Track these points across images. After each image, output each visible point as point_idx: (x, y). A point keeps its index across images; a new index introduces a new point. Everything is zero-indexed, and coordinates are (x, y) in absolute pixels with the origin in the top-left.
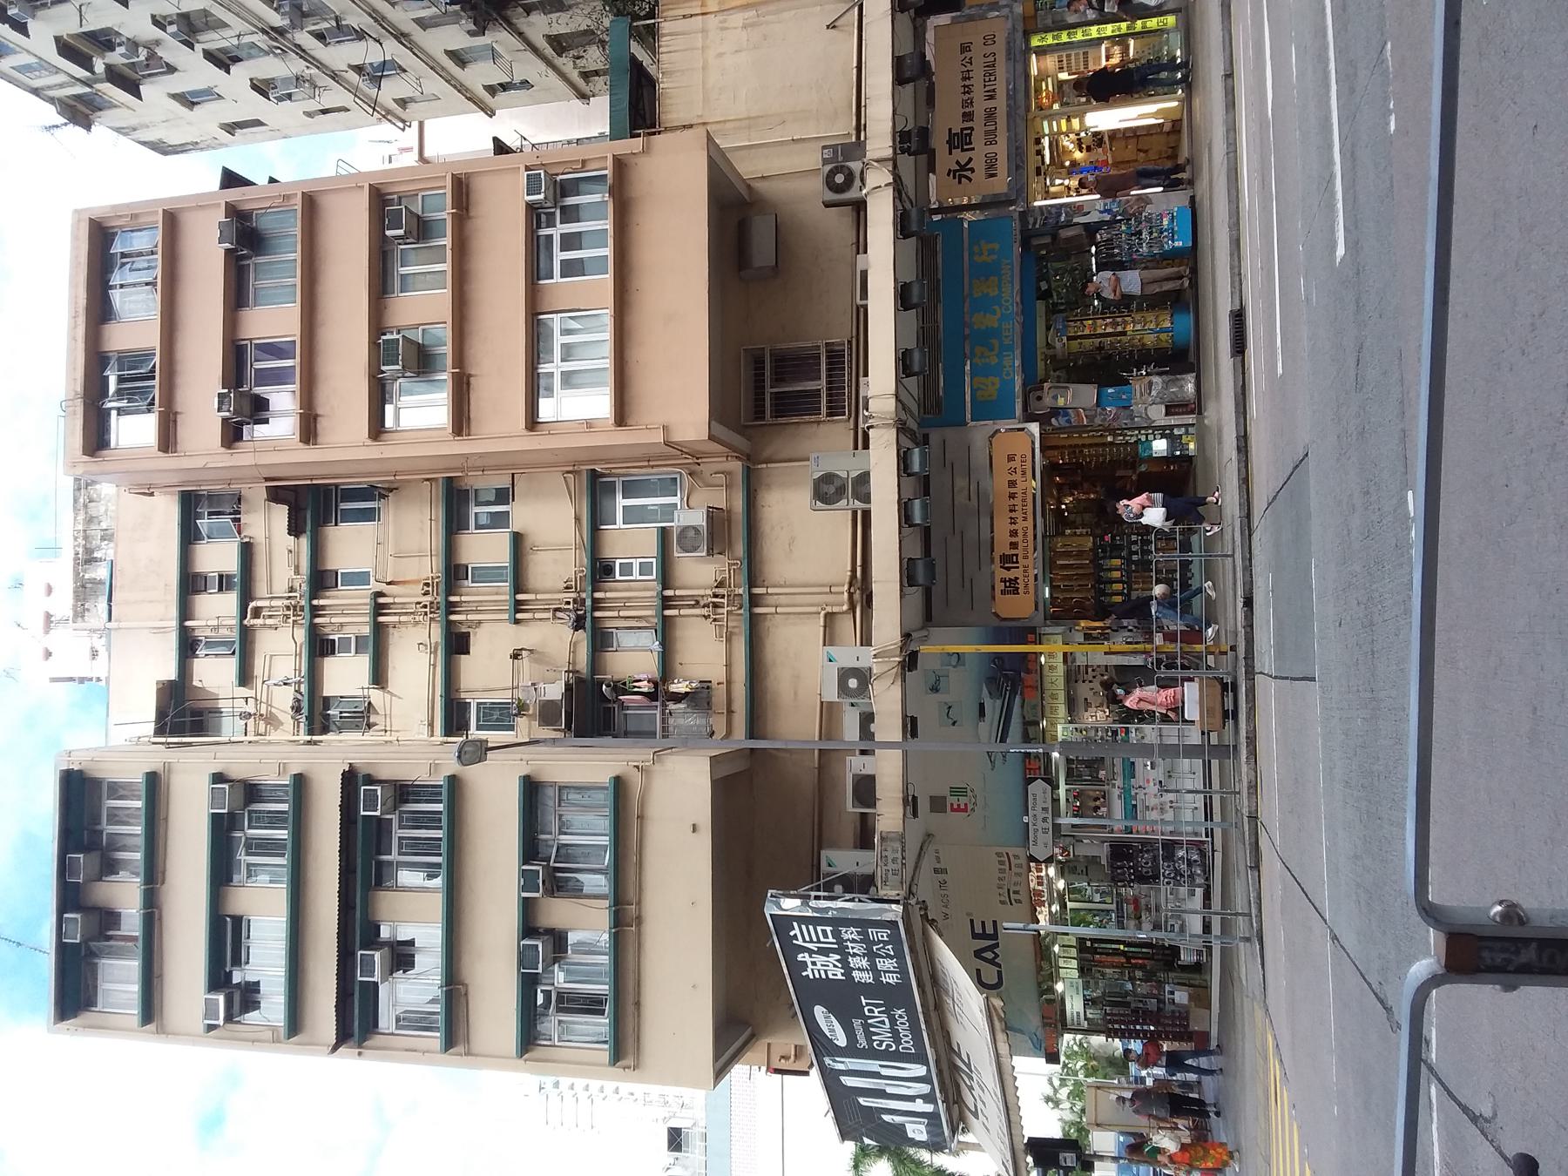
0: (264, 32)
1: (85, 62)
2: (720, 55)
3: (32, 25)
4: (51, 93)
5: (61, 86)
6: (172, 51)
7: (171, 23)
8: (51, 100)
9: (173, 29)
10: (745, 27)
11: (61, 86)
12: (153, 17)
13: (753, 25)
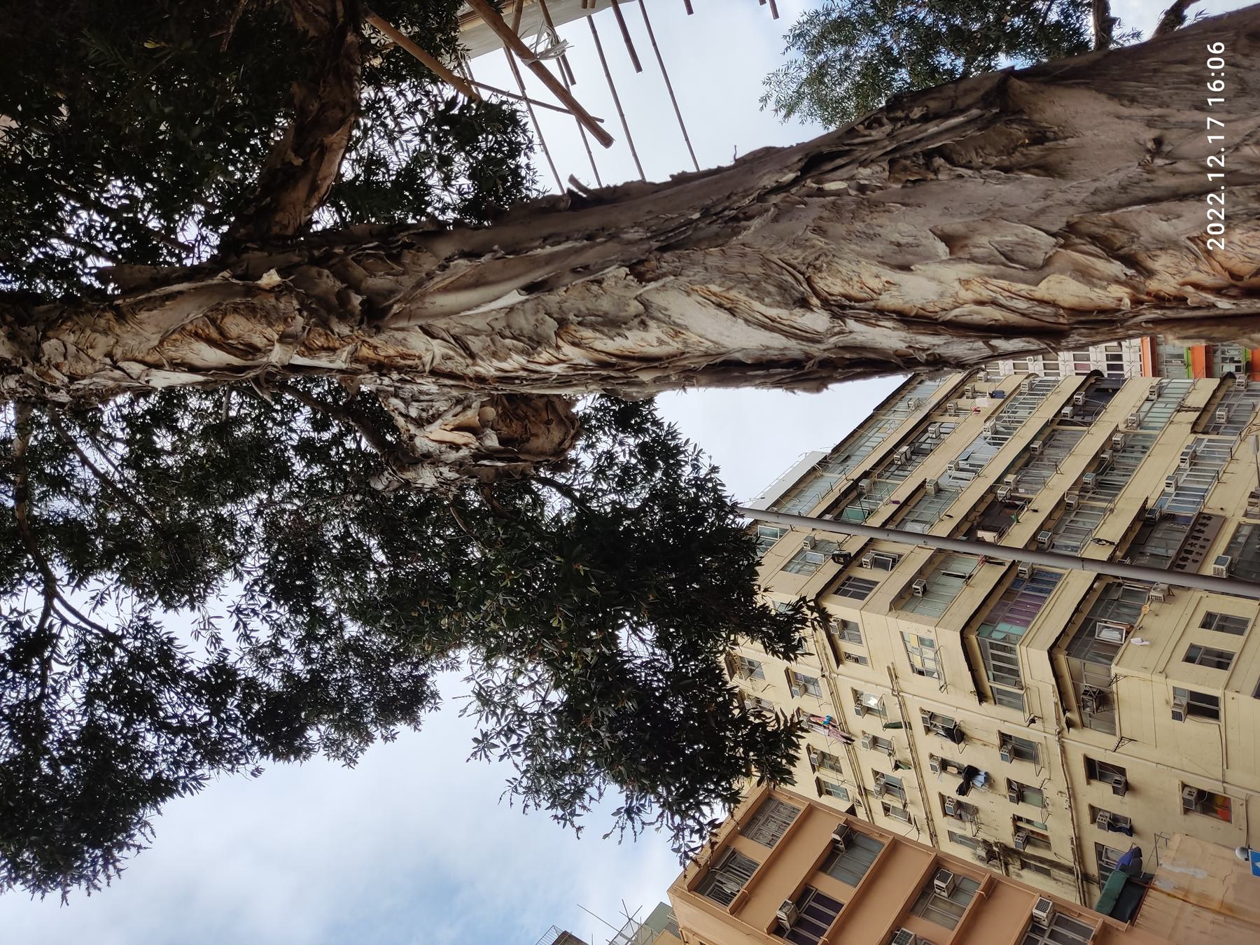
9: (813, 756)
10: (1213, 922)
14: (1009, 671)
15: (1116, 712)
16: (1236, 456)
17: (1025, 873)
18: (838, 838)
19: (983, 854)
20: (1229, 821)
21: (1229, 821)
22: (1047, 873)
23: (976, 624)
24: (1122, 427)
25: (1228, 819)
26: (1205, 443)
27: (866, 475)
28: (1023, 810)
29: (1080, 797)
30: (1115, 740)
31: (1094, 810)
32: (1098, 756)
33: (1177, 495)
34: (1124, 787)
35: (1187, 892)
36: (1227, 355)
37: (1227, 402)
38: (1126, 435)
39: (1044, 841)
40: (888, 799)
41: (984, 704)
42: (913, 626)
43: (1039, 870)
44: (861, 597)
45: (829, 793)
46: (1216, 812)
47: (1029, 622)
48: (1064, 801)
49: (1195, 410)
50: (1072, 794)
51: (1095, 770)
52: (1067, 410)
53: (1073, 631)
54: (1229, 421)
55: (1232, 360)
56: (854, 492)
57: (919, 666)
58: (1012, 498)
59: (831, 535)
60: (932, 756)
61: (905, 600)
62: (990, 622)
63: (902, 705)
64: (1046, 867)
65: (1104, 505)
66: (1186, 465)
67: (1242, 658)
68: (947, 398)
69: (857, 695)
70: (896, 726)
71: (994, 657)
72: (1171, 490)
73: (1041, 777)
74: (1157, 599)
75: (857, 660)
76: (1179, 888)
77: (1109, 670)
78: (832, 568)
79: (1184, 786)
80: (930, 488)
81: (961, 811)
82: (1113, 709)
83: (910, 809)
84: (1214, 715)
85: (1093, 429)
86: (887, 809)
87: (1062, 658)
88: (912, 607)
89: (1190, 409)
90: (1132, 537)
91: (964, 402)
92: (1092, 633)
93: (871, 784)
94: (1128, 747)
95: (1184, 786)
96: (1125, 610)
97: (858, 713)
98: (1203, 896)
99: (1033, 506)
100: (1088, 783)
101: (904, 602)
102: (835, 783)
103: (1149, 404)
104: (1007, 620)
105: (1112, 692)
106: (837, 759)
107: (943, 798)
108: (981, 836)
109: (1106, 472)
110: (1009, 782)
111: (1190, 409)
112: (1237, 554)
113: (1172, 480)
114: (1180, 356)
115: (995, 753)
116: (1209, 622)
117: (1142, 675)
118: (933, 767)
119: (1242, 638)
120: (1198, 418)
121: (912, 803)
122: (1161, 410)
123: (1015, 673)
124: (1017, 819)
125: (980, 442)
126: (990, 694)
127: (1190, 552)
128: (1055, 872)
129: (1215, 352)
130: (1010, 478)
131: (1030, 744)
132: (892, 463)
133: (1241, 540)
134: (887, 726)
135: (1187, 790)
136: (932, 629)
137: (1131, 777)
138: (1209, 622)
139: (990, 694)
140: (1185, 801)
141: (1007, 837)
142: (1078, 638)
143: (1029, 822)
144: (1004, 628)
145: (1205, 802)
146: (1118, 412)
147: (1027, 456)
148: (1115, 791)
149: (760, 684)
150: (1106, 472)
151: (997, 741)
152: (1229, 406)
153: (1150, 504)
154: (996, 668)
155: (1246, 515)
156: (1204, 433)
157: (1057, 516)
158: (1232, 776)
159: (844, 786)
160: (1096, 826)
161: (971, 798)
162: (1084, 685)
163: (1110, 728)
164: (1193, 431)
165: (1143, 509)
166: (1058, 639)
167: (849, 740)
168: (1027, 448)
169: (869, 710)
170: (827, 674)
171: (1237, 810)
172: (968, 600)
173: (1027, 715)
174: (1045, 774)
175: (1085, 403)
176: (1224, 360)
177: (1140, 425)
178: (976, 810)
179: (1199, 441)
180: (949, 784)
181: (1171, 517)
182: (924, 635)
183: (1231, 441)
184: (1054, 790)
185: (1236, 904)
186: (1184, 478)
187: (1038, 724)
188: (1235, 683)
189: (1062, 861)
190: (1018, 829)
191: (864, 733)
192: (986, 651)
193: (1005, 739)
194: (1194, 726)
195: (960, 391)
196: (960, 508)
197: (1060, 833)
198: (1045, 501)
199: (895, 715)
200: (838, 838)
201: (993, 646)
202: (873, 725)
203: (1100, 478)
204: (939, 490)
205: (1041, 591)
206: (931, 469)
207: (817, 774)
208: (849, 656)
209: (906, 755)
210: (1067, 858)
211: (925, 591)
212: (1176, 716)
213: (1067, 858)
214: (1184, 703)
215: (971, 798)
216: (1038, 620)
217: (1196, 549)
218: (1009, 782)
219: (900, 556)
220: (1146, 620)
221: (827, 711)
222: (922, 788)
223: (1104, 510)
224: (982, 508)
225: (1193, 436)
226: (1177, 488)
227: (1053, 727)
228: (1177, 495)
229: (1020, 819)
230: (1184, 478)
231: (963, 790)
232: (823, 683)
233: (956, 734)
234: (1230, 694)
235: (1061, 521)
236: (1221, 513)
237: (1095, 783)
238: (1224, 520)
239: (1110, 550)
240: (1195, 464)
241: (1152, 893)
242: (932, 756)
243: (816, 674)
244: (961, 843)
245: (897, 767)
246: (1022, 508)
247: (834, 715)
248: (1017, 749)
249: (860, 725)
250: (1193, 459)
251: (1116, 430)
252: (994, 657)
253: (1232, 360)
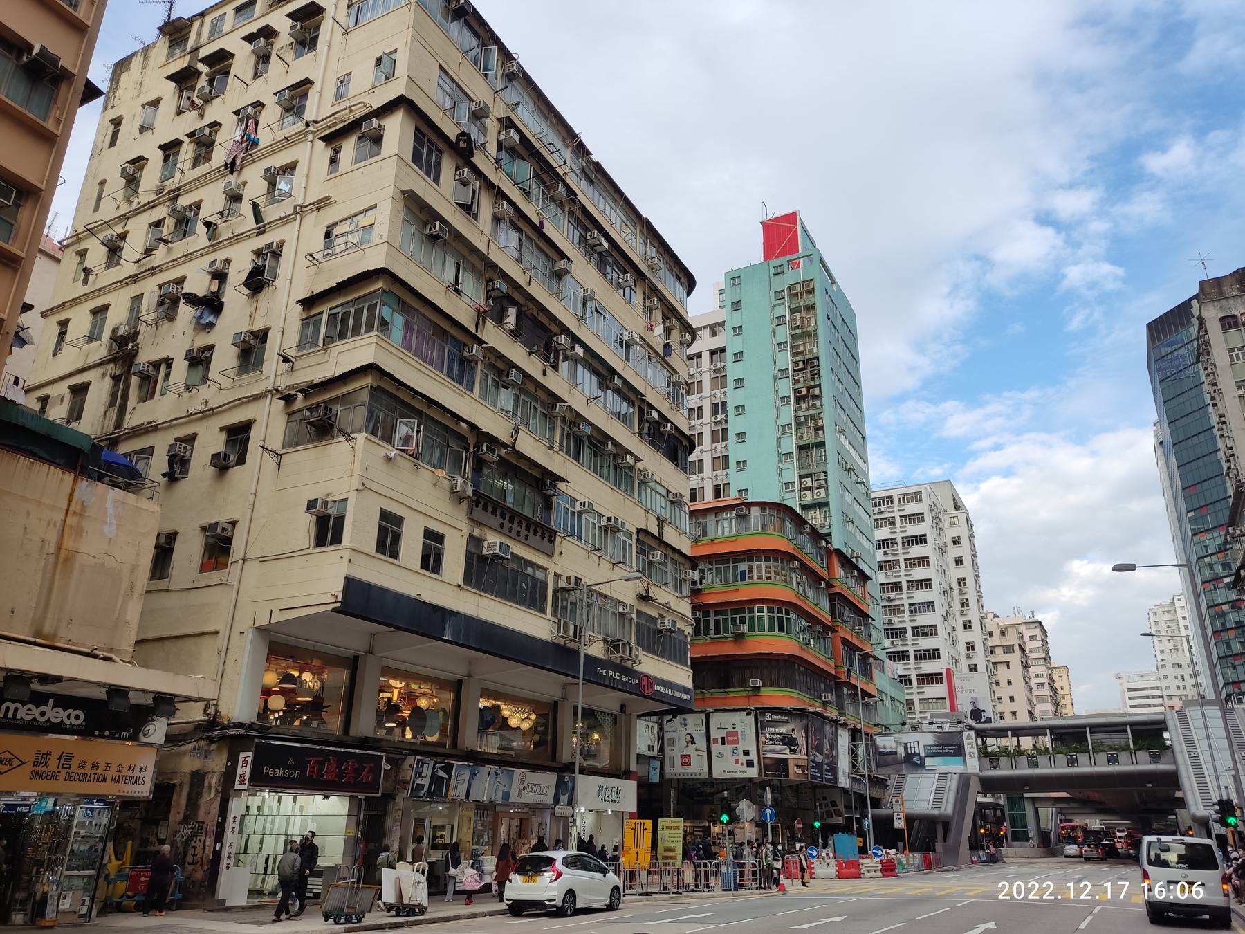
0: (178, 189)
1: (208, 60)
2: (28, 514)
3: (248, 47)
4: (196, 25)
5: (199, 34)
6: (190, 121)
7: (211, 133)
8: (192, 19)
9: (207, 131)
10: (43, 541)
11: (199, 34)
12: (220, 125)
13: (42, 548)
14: (342, 329)
15: (311, 445)
16: (616, 568)
17: (108, 381)
18: (36, 51)
19: (121, 332)
20: (201, 570)
21: (201, 570)
22: (112, 403)
23: (397, 290)
24: (639, 465)
25: (202, 569)
26: (628, 541)
27: (571, 192)
28: (180, 369)
29: (205, 423)
30: (277, 447)
31: (191, 439)
32: (256, 435)
33: (573, 513)
34: (222, 465)
35: (81, 515)
36: (707, 574)
37: (669, 562)
38: (631, 468)
39: (148, 392)
40: (170, 223)
41: (299, 308)
42: (385, 217)
43: (114, 395)
44: (417, 158)
45: (166, 159)
46: (210, 558)
47: (409, 349)
48: (197, 406)
49: (660, 533)
50: (207, 413)
51: (239, 435)
52: (655, 415)
53: (401, 395)
54: (650, 563)
55: (702, 578)
56: (547, 174)
57: (336, 231)
58: (557, 352)
59: (490, 137)
60: (228, 261)
61: (417, 209)
62: (403, 307)
63: (285, 220)
64: (118, 402)
65: (557, 439)
66: (604, 522)
67: (392, 567)
68: (663, 300)
69: (290, 169)
70: (258, 216)
71: (359, 312)
72: (578, 507)
73: (221, 379)
74: (455, 485)
75: (333, 161)
76: (84, 507)
77: (360, 431)
78: (452, 132)
79: (234, 524)
80: (562, 265)
81: (169, 303)
82: (313, 442)
83: (162, 249)
84: (320, 541)
85: (636, 438)
86: (158, 224)
87: (368, 381)
88: (411, 230)
89: (660, 529)
90: (523, 465)
91: (657, 315)
92: (403, 416)
93: (184, 201)
94: (271, 462)
95: (234, 524)
96: (437, 453)
97: (267, 170)
98: (79, 532)
99: (550, 372)
100: (222, 429)
101: (416, 211)
102: (181, 158)
103: (663, 492)
104: (407, 326)
105: (333, 438)
106: (208, 159)
107: (180, 281)
108: (142, 328)
109: (593, 446)
110: (211, 348)
111: (660, 529)
112: (514, 566)
113: (587, 508)
114: (705, 533)
115: (244, 327)
116: (433, 538)
117: (357, 465)
118: (213, 263)
119: (417, 567)
120: (653, 535)
121: (169, 250)
122: (660, 505)
123: (343, 336)
124: (168, 362)
125: (616, 328)
126: (314, 312)
127: (511, 521)
128: (114, 412)
129: (710, 563)
130: (580, 351)
131: (259, 364)
132: (587, 230)
133: (530, 570)
134: (255, 206)
135: (229, 527)
136: (385, 239)
137: (236, 472)
138: (433, 538)
139: (314, 312)
140: (213, 526)
141: (145, 356)
142: (391, 402)
143: (167, 376)
144: (398, 322)
145: (218, 546)
146: (654, 463)
147: (604, 372)
148: (215, 457)
149: (289, 55)
150: (593, 446)
151: (257, 326)
152: (665, 564)
153: (560, 485)
154: (345, 317)
155: (556, 575)
156: (638, 540)
157: (540, 393)
158: (252, 569)
159: (178, 173)
160: (172, 442)
161: (186, 312)
162: (338, 408)
163: (292, 442)
164: (639, 531)
165: (556, 478)
166: (391, 377)
167: (231, 167)
168: (613, 372)
169: (272, 185)
170: (311, 128)
171: (215, 577)
172: (431, 279)
173: (294, 354)
174: (225, 383)
175: (662, 434)
176: (703, 571)
177: (643, 483)
178: (172, 319)
179: (630, 536)
180: (199, 284)
181: (548, 505)
182: (376, 230)
183: (631, 561)
184: (208, 394)
185: (77, 565)
186: (591, 520)
187: (284, 367)
188: (360, 559)
189: (127, 416)
190: (156, 365)
191: (245, 184)
192: (364, 302)
193: (262, 336)
194: (305, 524)
195: (670, 315)
196: (538, 291)
197: (161, 408)
198: (556, 382)
199: (271, 213)
200: (36, 51)
201: (372, 308)
202: (255, 186)
203: (586, 440)
204: (559, 276)
205: (450, 368)
206: (583, 271)
207: (186, 140)
208: (337, 151)
209: (225, 232)
210: (131, 421)
211: (434, 238)
212: (312, 504)
213: (131, 421)
214: (329, 511)
215: (186, 312)
216: (411, 359)
217: (515, 527)
218: (211, 348)
219: (476, 217)
220: (426, 474)
221: (264, 137)
222: (188, 257)
223: (551, 440)
224: (542, 318)
225: (634, 531)
226: (580, 513)
227: (283, 383)
228: (573, 513)
229: (169, 366)
230: (591, 520)
231: (192, 299)
232: (300, 126)
233: (257, 282)
234: (347, 554)
235: (536, 399)
236: (557, 552)
237: (223, 436)
238: (551, 556)
239: (507, 441)
240: (606, 532)
241: (69, 477)
242: (228, 261)
243: (309, 115)
244: (132, 309)
245: (208, 225)
246: (546, 359)
247: (261, 145)
248: (251, 349)
249: (253, 181)
250: (611, 529)
251: (637, 459)
252: (359, 312)
253: (702, 578)
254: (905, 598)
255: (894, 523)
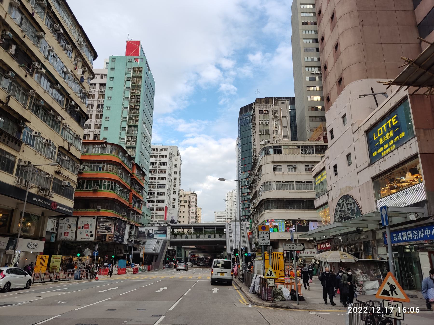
16: (47, 160)
24: (64, 121)
26: (54, 150)
33: (31, 136)
37: (71, 160)
38: (60, 122)
49: (69, 149)
54: (63, 160)
55: (84, 168)
65: (28, 104)
66: (45, 141)
68: (83, 59)
72: (33, 133)
80: (41, 34)
85: (64, 111)
89: (69, 147)
91: (80, 65)
99: (29, 76)
103: (72, 133)
111: (69, 147)
113: (38, 135)
114: (87, 152)
120: (65, 149)
122: (70, 138)
125: (61, 65)
129: (88, 163)
130: (44, 71)
132: (54, 23)
133: (7, 156)
146: (70, 122)
147: (54, 82)
152: (69, 161)
153: (27, 124)
164: (60, 147)
165: (25, 120)
168: (57, 82)
175: (75, 111)
176: (84, 165)
177: (64, 129)
181: (20, 131)
186: (39, 140)
195: (85, 66)
196: (28, 42)
198: (31, 81)
203: (41, 107)
204: (39, 38)
206: (50, 39)
223: (25, 104)
225: (57, 146)
226: (34, 136)
228: (31, 136)
230: (39, 140)
235: (21, 86)
236: (21, 150)
240: (45, 145)
246: (28, 70)
250: (48, 144)
251: (63, 119)
253: (84, 168)
254: (155, 198)
255: (156, 179)
